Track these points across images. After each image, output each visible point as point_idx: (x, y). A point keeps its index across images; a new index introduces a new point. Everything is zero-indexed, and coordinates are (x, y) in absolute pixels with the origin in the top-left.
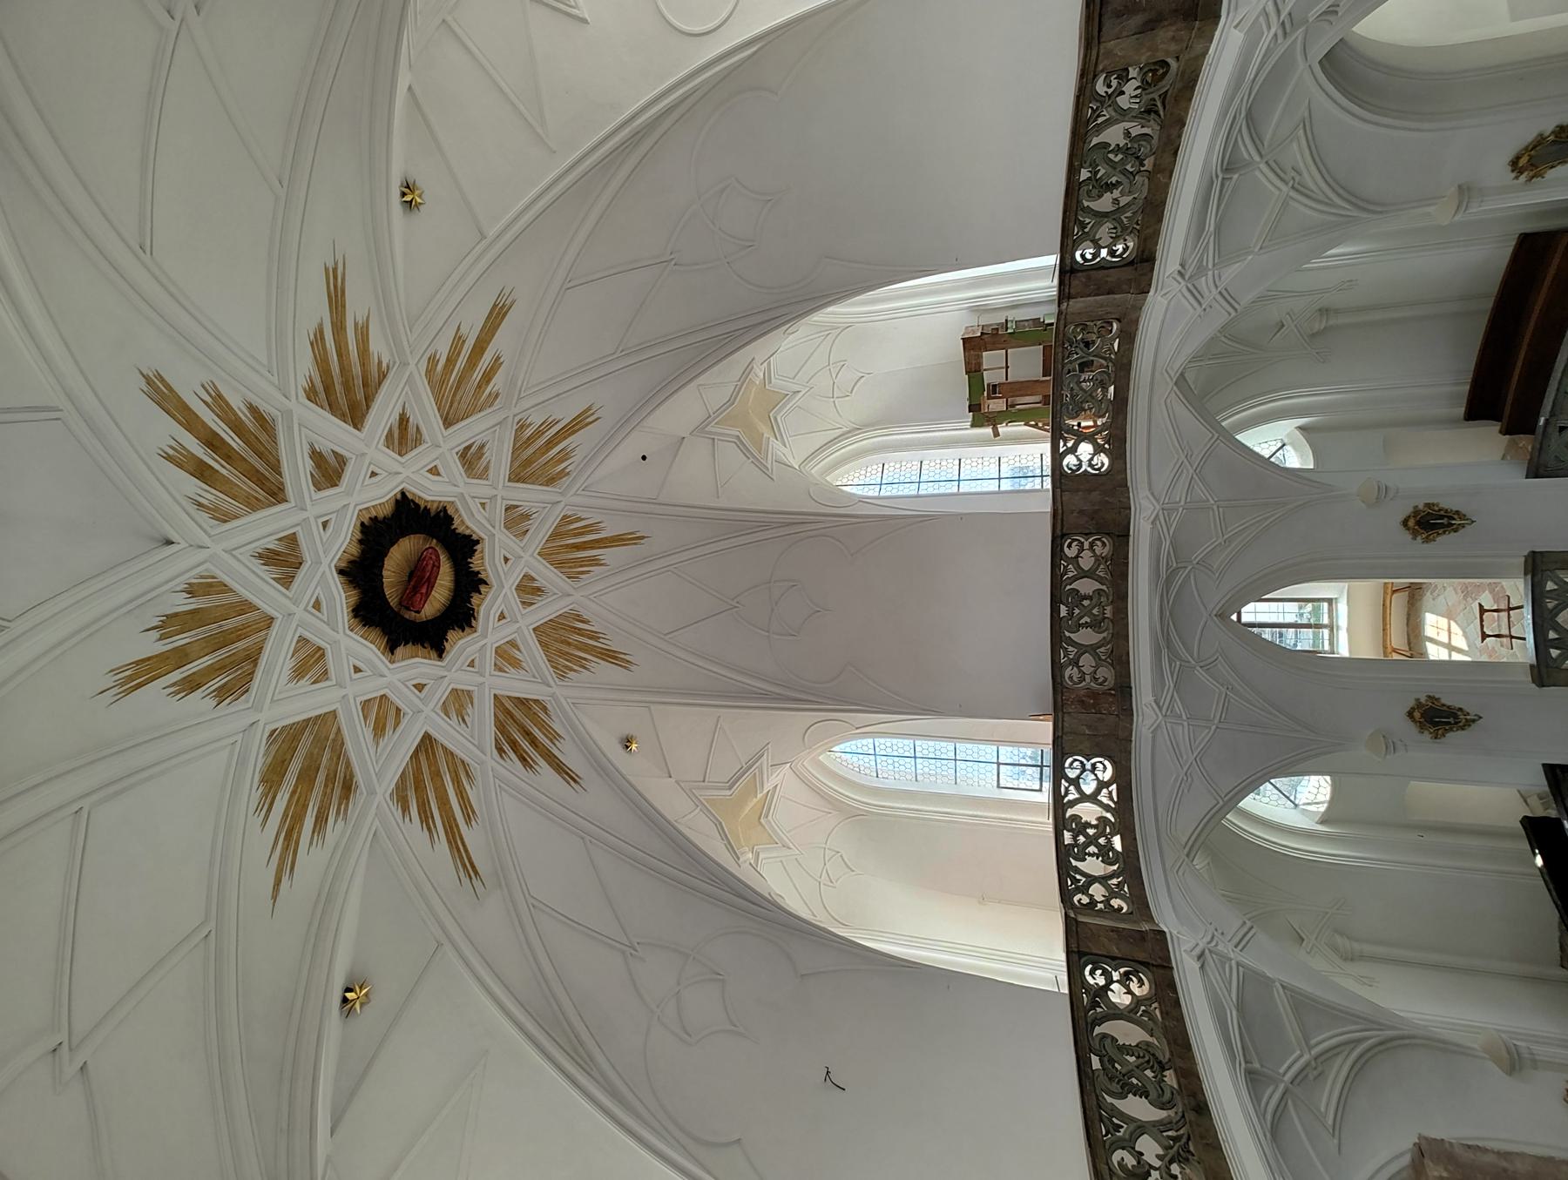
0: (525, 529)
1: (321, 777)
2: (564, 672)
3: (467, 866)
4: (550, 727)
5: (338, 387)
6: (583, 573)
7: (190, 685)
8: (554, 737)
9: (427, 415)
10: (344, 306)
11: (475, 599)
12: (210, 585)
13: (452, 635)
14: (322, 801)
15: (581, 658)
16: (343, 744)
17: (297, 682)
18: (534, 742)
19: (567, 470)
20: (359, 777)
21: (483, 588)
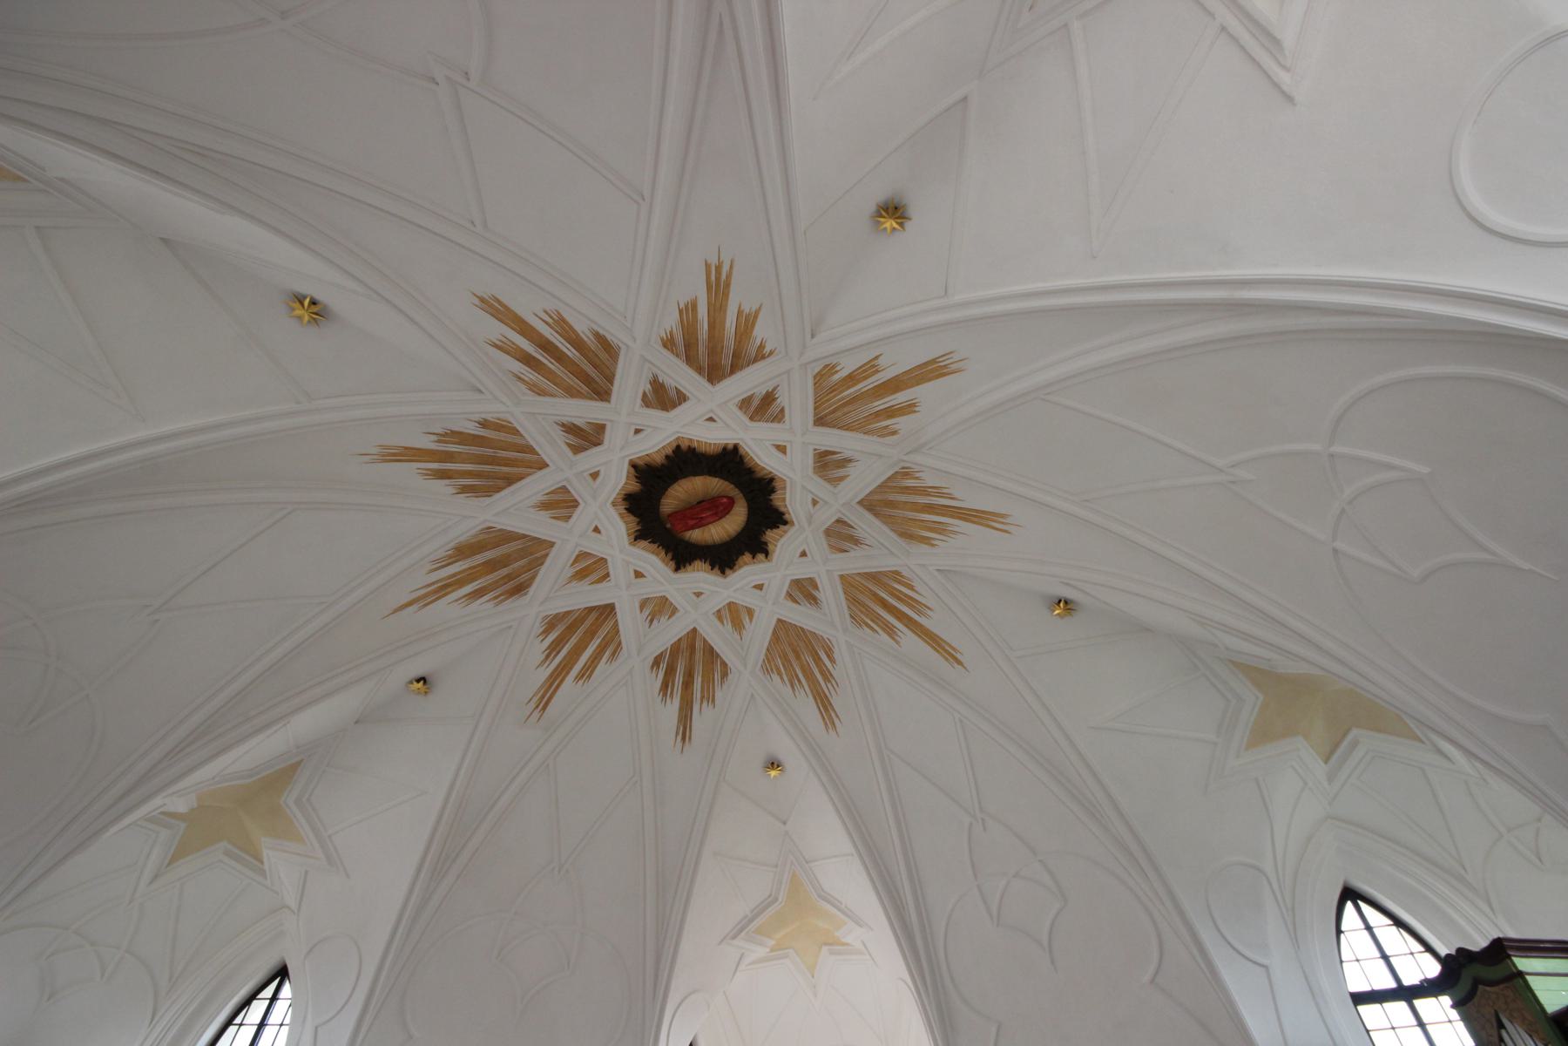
0: (844, 548)
1: (505, 571)
2: (772, 670)
6: (867, 625)
8: (708, 696)
10: (726, 295)
11: (747, 557)
12: (503, 426)
13: (698, 564)
14: (490, 585)
15: (797, 676)
16: (542, 564)
18: (688, 685)
20: (532, 590)
21: (761, 556)
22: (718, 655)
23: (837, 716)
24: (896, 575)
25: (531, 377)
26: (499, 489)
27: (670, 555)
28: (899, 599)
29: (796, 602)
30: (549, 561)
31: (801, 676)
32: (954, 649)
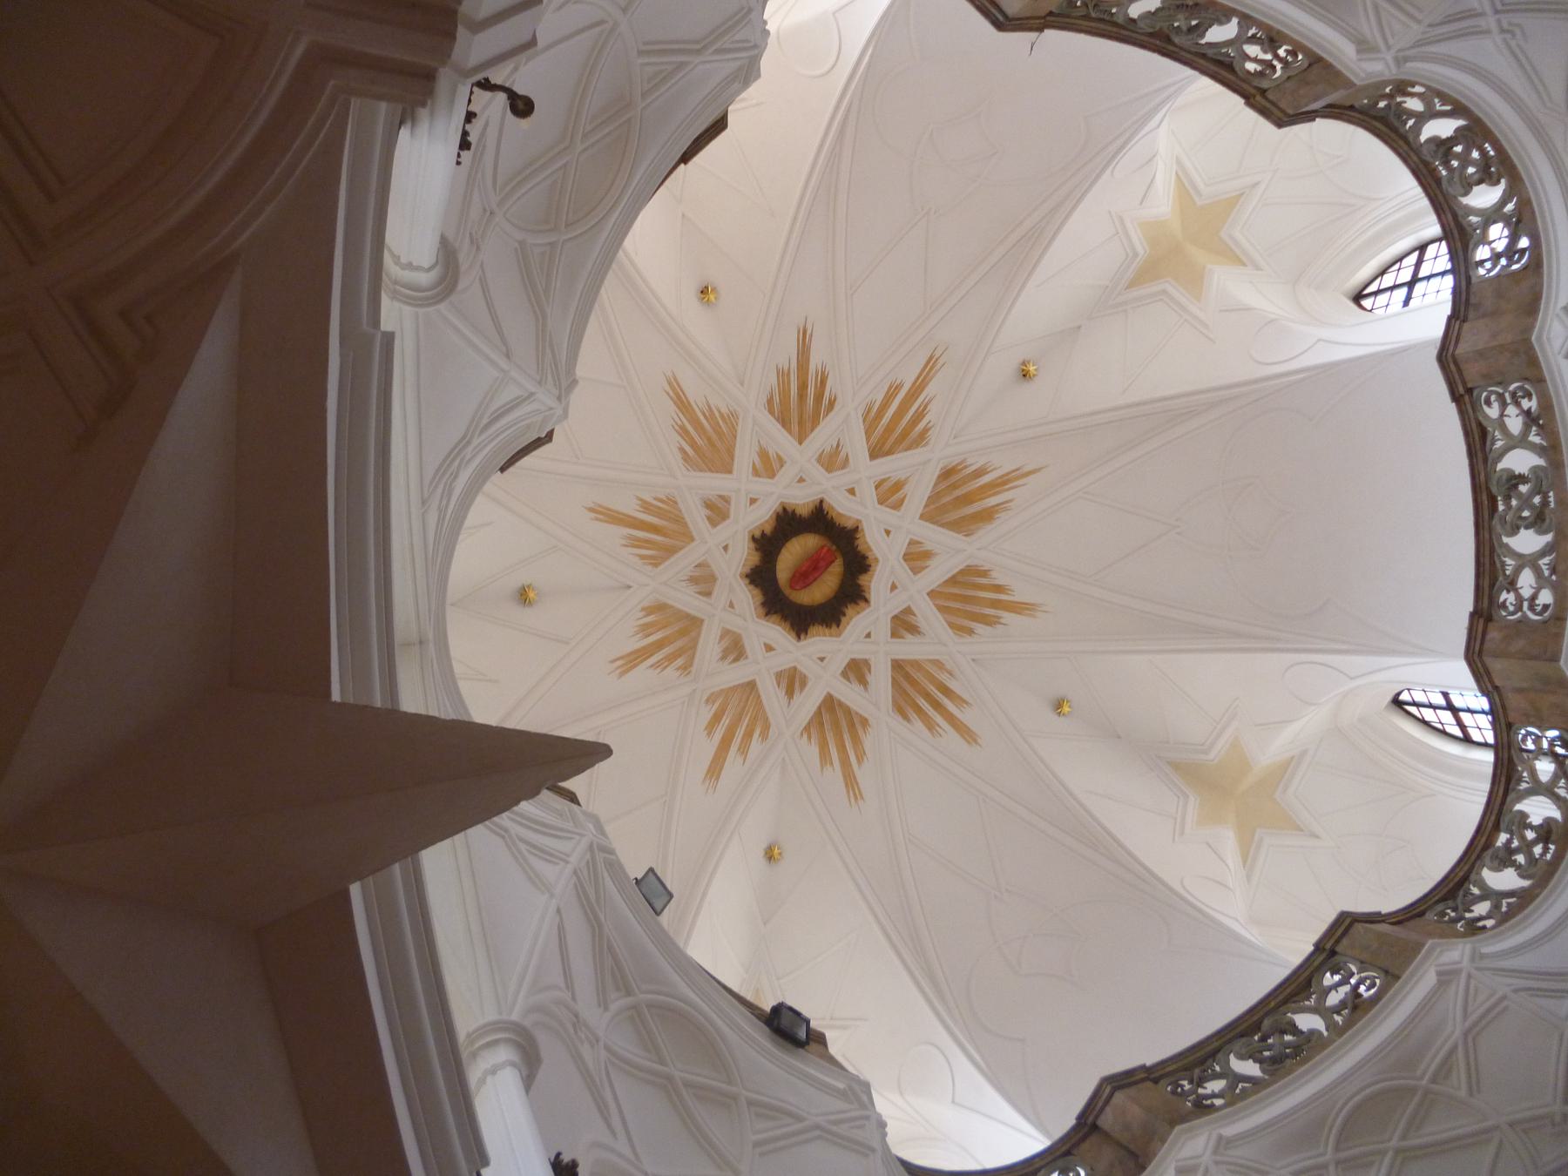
3: (930, 367)
4: (779, 384)
5: (844, 724)
7: (999, 589)
8: (783, 375)
9: (772, 695)
10: (845, 776)
11: (768, 530)
13: (804, 511)
14: (969, 481)
16: (929, 497)
18: (803, 387)
19: (644, 613)
20: (937, 473)
21: (758, 534)
22: (778, 420)
23: (668, 394)
24: (655, 562)
26: (962, 572)
27: (829, 516)
28: (647, 541)
29: (720, 496)
30: (924, 503)
31: (702, 418)
32: (597, 519)
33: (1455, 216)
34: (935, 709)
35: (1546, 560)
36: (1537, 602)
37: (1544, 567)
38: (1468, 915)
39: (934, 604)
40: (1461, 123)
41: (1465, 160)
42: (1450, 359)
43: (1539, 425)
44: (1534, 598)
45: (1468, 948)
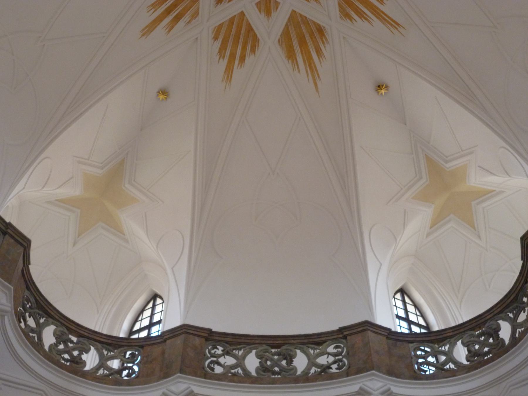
7: (243, 59)
16: (306, 18)
17: (271, 17)
20: (322, 24)
25: (187, 17)
26: (255, 35)
30: (303, 13)
33: (451, 337)
34: (166, 10)
35: (240, 371)
36: (216, 365)
37: (236, 370)
38: (27, 314)
39: (235, 16)
40: (507, 342)
41: (483, 344)
42: (365, 328)
43: (321, 372)
44: (219, 364)
45: (8, 309)
